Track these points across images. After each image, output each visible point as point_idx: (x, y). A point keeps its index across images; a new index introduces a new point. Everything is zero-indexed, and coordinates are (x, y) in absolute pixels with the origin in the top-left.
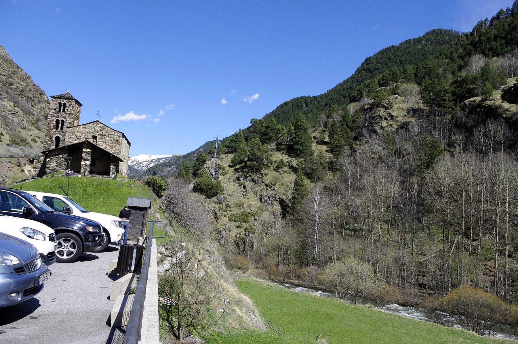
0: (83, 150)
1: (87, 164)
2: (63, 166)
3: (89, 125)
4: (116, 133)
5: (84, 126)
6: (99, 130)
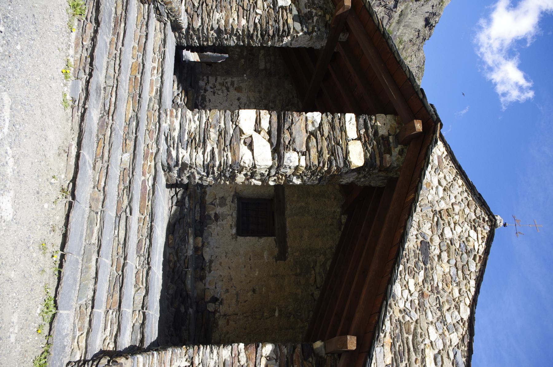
0: (350, 117)
1: (244, 150)
2: (217, 16)
3: (460, 182)
4: (455, 338)
5: (445, 163)
6: (448, 234)
